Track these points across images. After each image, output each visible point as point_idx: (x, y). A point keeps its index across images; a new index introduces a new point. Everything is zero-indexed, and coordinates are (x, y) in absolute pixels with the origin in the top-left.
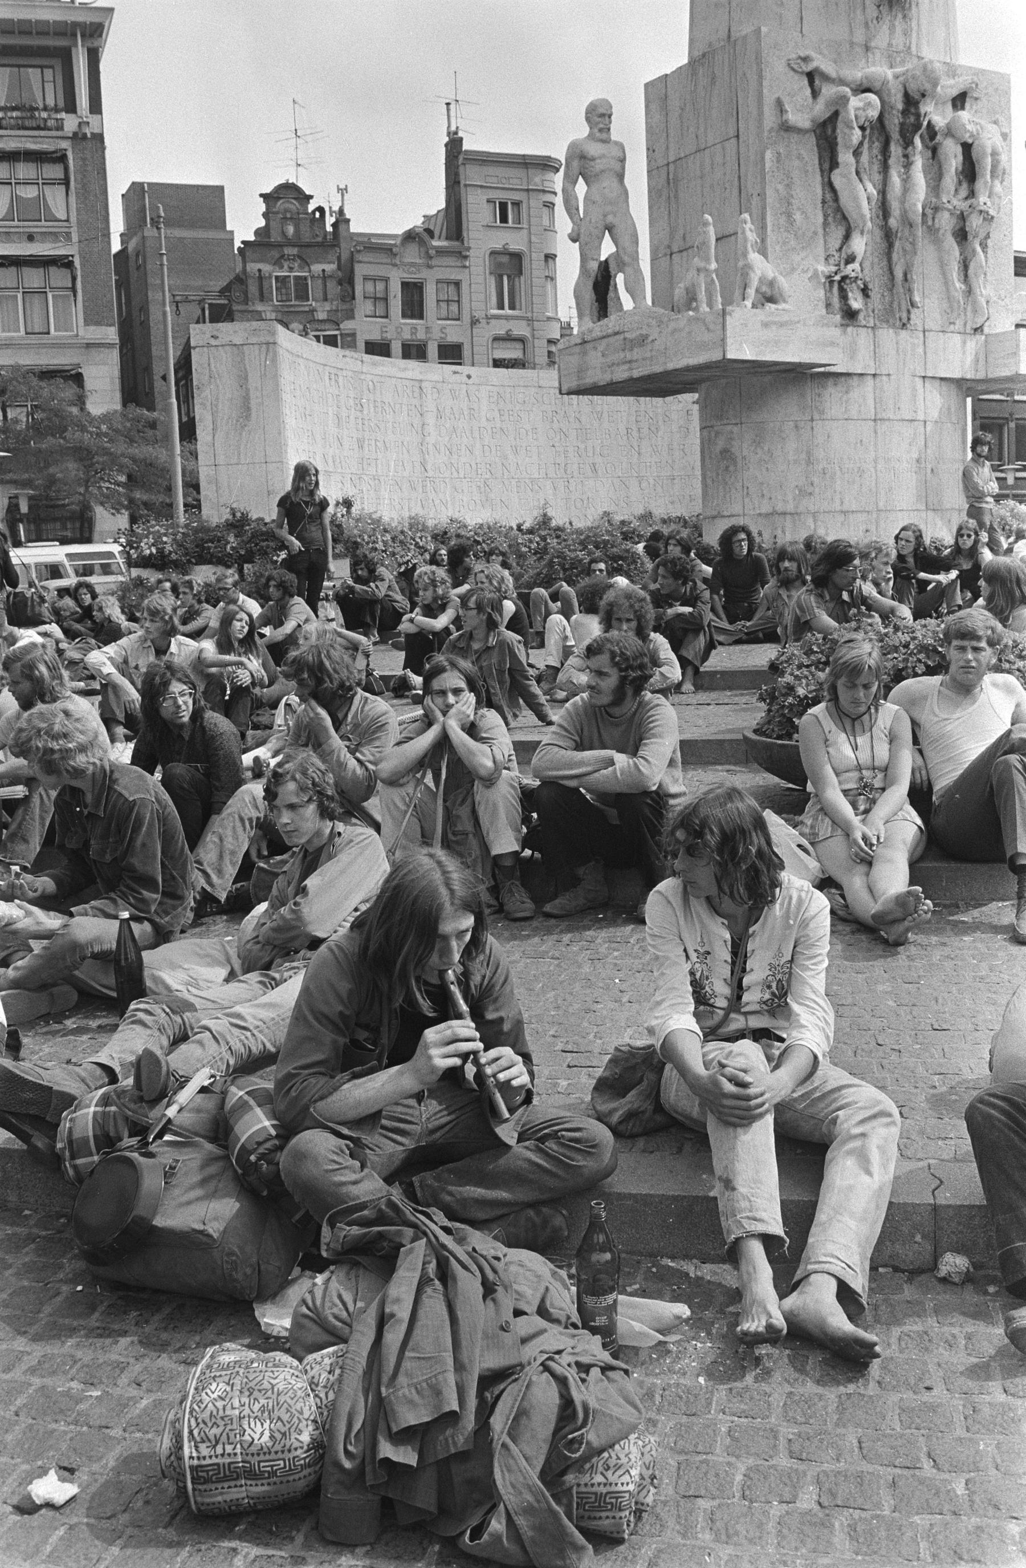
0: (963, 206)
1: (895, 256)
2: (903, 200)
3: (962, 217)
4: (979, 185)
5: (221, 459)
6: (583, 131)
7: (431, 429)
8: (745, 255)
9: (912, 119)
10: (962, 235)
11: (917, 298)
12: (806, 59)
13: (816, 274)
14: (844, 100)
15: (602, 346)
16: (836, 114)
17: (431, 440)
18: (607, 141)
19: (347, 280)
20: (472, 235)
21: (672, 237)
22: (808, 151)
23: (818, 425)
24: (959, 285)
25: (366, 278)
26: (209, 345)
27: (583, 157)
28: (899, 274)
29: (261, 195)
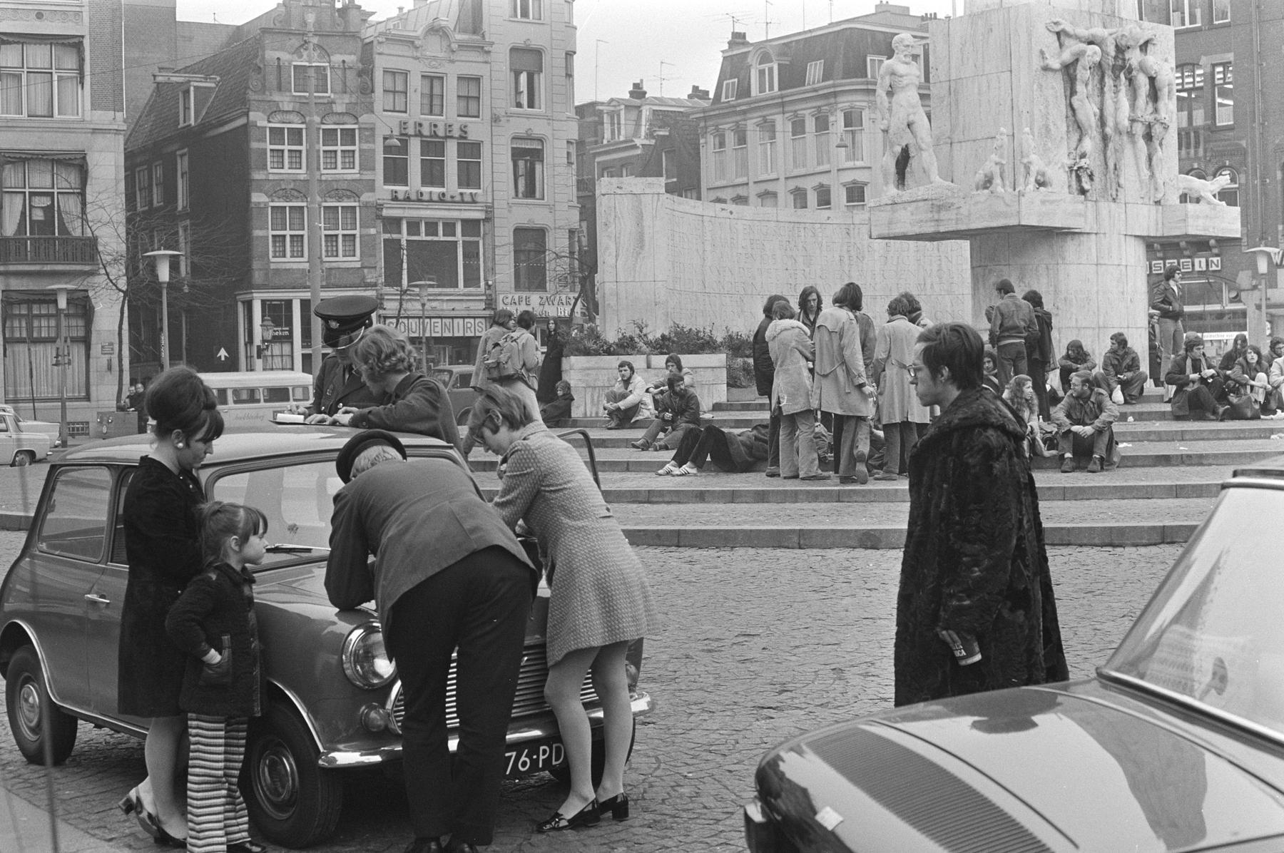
0: (1150, 118)
1: (1109, 153)
3: (1149, 126)
4: (1161, 105)
9: (1120, 62)
10: (1149, 137)
11: (1122, 181)
12: (1056, 23)
13: (1063, 166)
14: (1082, 53)
15: (911, 208)
16: (1077, 60)
19: (366, 71)
21: (952, 131)
22: (1056, 84)
23: (1061, 267)
26: (615, 194)
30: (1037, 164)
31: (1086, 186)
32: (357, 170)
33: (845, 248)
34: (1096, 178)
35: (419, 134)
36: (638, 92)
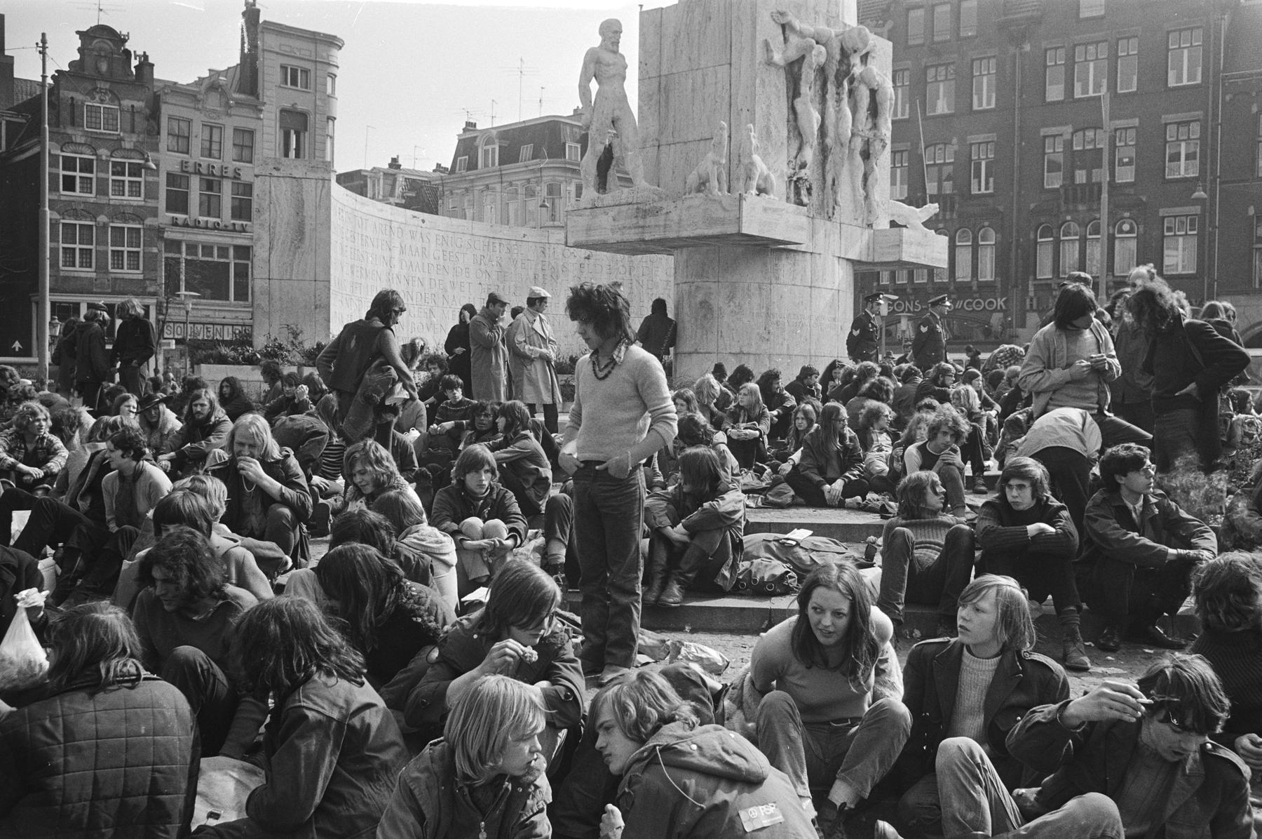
0: (870, 134)
1: (828, 167)
2: (837, 127)
5: (275, 275)
6: (596, 41)
7: (396, 262)
8: (750, 155)
10: (866, 155)
11: (839, 199)
12: (782, 14)
15: (613, 212)
16: (803, 57)
17: (396, 270)
18: (616, 52)
19: (154, 115)
20: (268, 93)
21: (661, 132)
22: (779, 82)
24: (862, 191)
25: (170, 118)
26: (271, 176)
27: (598, 62)
28: (829, 182)
29: (78, 32)
30: (760, 166)
31: (805, 200)
32: (142, 198)
33: (540, 267)
34: (814, 192)
35: (200, 173)
36: (395, 163)
